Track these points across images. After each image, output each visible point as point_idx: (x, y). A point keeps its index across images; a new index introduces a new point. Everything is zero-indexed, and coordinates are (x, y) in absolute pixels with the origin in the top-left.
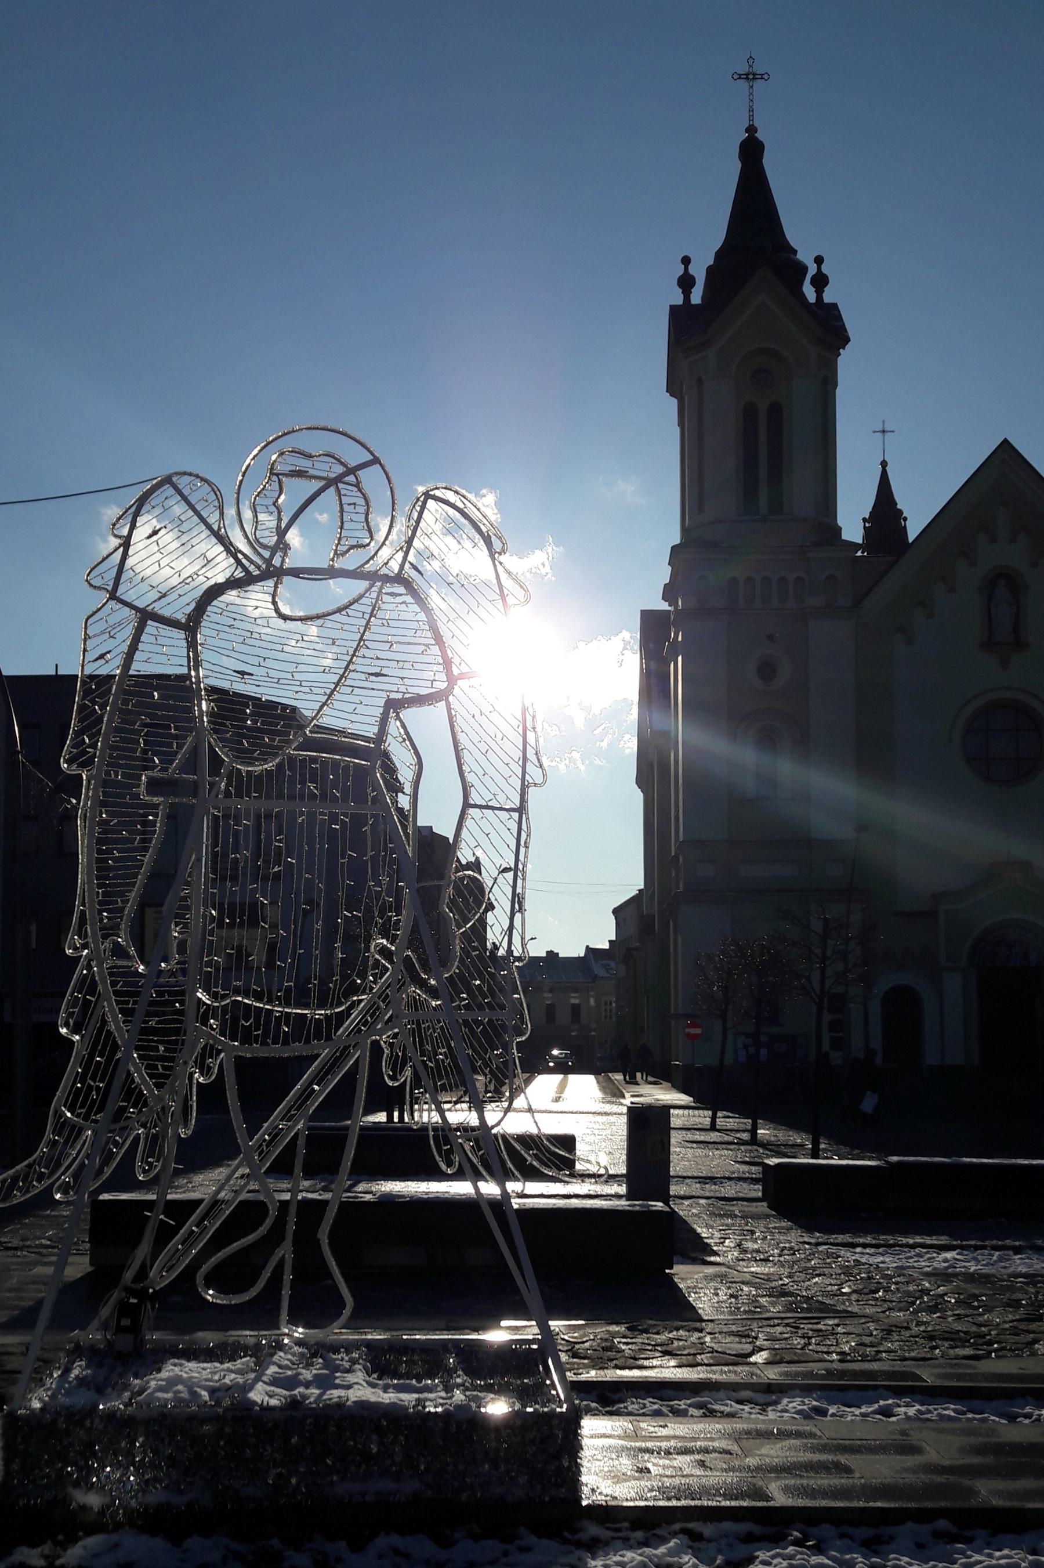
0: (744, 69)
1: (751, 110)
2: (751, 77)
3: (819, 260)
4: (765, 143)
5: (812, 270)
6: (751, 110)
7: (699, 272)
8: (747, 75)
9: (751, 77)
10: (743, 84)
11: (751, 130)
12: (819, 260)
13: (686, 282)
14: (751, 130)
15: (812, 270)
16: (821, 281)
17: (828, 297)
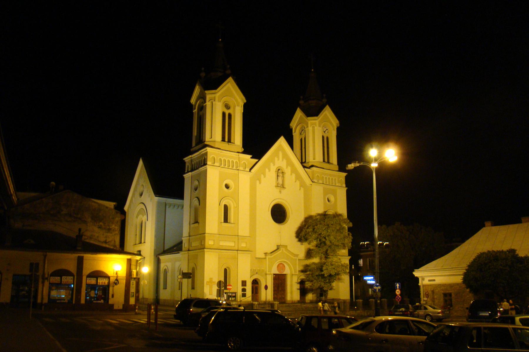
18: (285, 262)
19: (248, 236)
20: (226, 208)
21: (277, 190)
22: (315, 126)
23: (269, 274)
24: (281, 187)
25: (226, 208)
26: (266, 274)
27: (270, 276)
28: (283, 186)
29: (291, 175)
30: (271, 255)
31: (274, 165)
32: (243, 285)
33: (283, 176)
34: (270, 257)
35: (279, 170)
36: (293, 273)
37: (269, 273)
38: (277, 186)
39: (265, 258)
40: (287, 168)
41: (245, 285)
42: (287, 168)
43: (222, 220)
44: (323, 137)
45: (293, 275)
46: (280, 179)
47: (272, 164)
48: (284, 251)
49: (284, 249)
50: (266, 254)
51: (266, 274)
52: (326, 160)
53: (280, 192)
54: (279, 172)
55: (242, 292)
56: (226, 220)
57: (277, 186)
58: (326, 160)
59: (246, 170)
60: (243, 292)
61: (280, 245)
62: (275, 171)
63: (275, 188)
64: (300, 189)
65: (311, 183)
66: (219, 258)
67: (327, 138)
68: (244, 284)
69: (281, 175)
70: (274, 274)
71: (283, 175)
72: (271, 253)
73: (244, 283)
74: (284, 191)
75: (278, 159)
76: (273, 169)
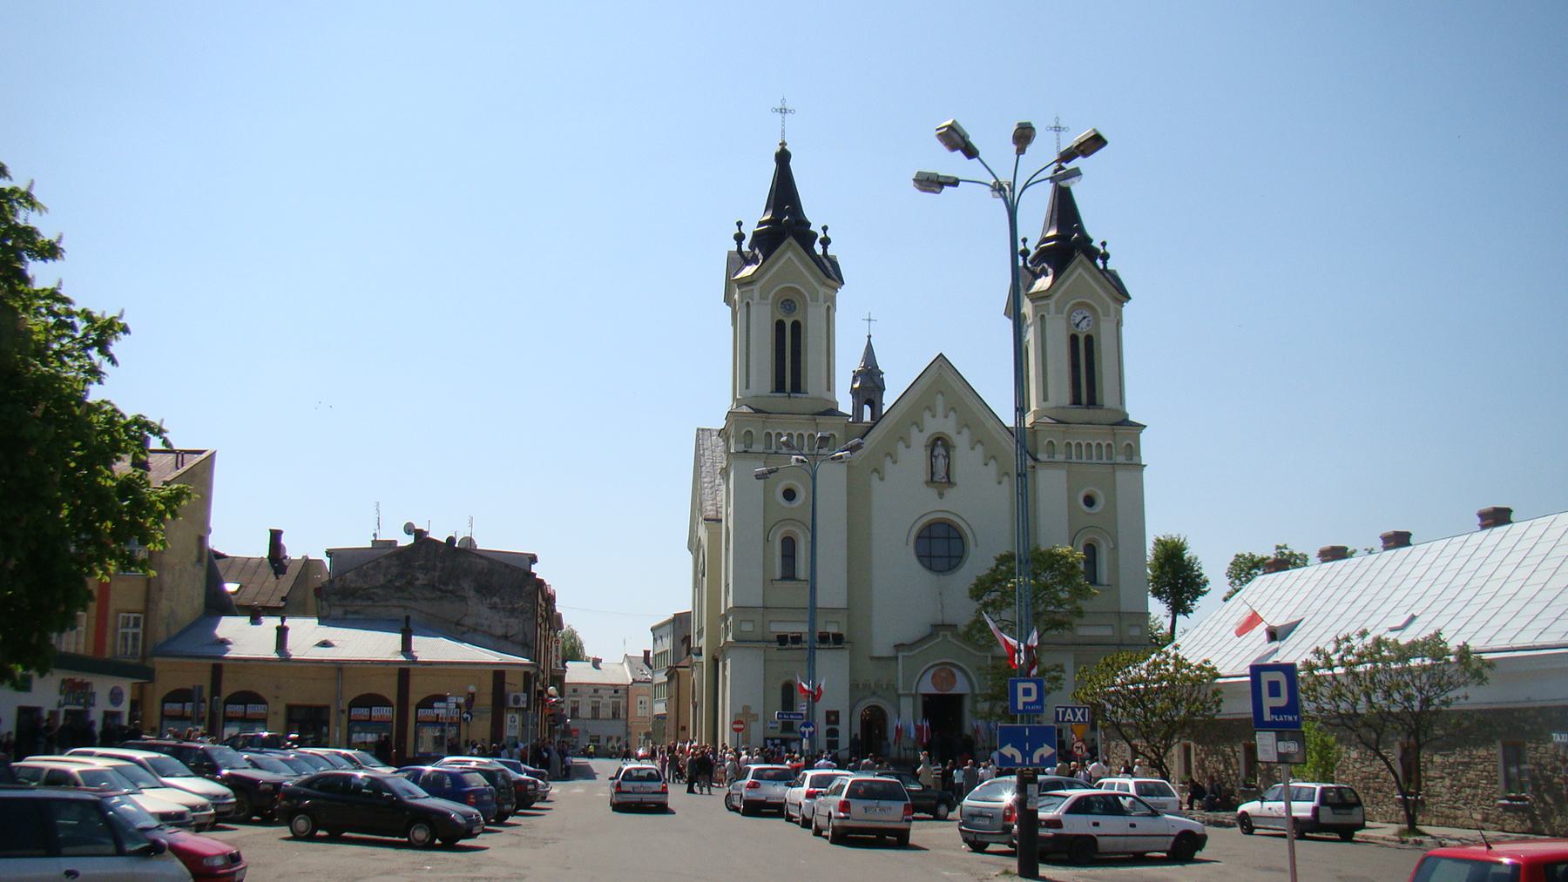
0: (779, 106)
1: (783, 131)
2: (783, 111)
3: (825, 229)
5: (821, 235)
6: (783, 131)
7: (749, 231)
8: (781, 109)
9: (783, 111)
10: (779, 115)
11: (783, 144)
12: (825, 229)
13: (739, 238)
14: (783, 144)
15: (821, 235)
16: (826, 242)
17: (830, 252)
18: (961, 669)
19: (845, 607)
20: (789, 545)
21: (932, 493)
22: (1045, 314)
23: (905, 695)
24: (941, 482)
25: (789, 545)
26: (899, 696)
27: (911, 699)
28: (949, 482)
29: (972, 448)
30: (911, 651)
32: (828, 722)
33: (948, 456)
34: (906, 654)
35: (938, 439)
36: (977, 692)
37: (906, 692)
39: (897, 657)
40: (959, 433)
41: (837, 722)
42: (959, 433)
43: (778, 574)
44: (1074, 339)
45: (976, 696)
46: (941, 463)
47: (914, 430)
48: (949, 636)
49: (948, 634)
50: (899, 647)
51: (899, 696)
53: (941, 495)
54: (939, 443)
55: (827, 736)
56: (789, 574)
57: (931, 481)
60: (829, 738)
61: (941, 623)
62: (925, 444)
63: (925, 486)
64: (1000, 483)
66: (765, 660)
67: (1089, 340)
68: (833, 718)
69: (940, 451)
70: (924, 695)
71: (948, 453)
72: (912, 644)
73: (833, 717)
74: (950, 493)
75: (934, 416)
76: (919, 440)
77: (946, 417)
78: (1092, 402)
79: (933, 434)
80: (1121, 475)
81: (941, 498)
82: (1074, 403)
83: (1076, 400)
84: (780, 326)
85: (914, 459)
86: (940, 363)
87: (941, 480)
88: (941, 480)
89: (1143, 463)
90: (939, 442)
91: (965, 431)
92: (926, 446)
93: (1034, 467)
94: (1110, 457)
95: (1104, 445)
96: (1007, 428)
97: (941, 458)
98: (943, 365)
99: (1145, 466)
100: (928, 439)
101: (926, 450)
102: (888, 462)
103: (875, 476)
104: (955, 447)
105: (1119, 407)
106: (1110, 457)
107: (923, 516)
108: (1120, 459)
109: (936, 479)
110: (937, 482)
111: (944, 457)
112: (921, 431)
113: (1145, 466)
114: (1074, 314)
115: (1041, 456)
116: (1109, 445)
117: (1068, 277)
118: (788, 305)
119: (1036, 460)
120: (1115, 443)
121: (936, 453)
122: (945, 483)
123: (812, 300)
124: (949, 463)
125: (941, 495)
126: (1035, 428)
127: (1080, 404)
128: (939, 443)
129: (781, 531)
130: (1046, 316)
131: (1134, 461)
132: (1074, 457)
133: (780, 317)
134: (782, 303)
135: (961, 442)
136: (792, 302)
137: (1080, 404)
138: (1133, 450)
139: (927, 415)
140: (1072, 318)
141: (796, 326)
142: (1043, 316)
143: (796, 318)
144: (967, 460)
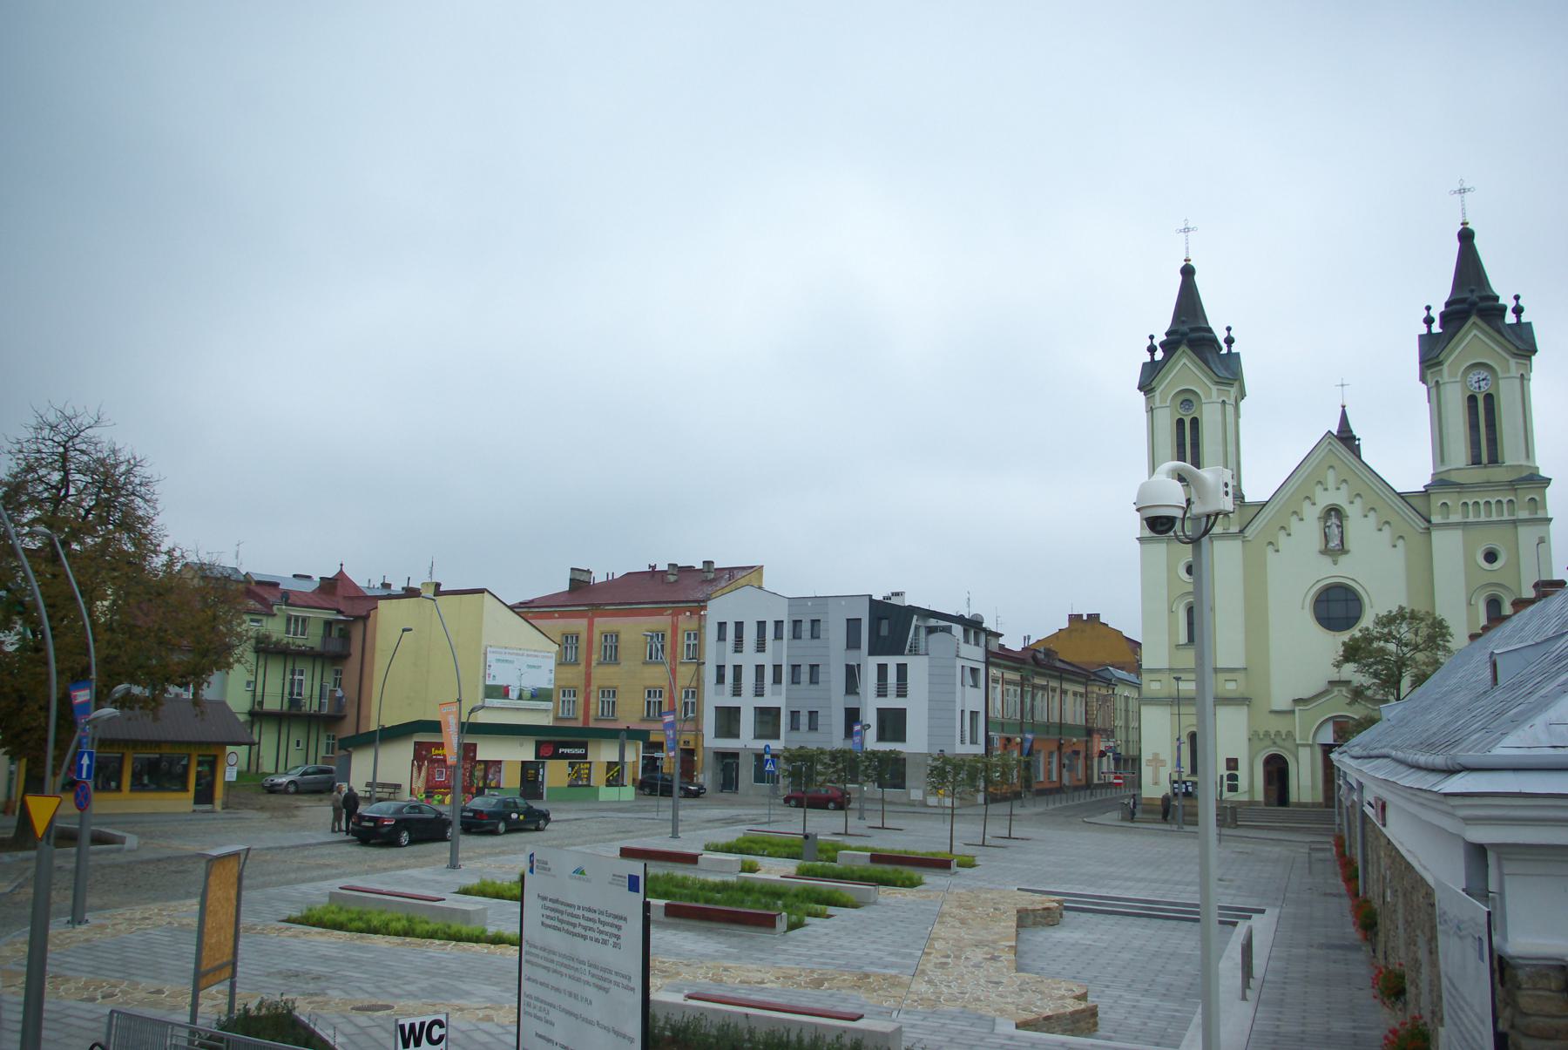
4: (1179, 269)
21: (1327, 560)
22: (1439, 379)
28: (1342, 549)
31: (1314, 504)
33: (1340, 526)
35: (1332, 509)
38: (1326, 551)
40: (1352, 503)
44: (1472, 399)
52: (1485, 458)
53: (1335, 563)
57: (1326, 551)
58: (1485, 458)
59: (1231, 531)
65: (1426, 525)
67: (1489, 398)
69: (1334, 520)
71: (1341, 523)
74: (1343, 559)
76: (1312, 513)
77: (1338, 489)
78: (1494, 459)
79: (1325, 507)
80: (1523, 531)
81: (1335, 564)
82: (1473, 464)
83: (1476, 461)
84: (1180, 422)
85: (1308, 531)
86: (1330, 440)
87: (1335, 549)
88: (1335, 549)
89: (1549, 516)
90: (1333, 513)
91: (1358, 501)
92: (1319, 518)
93: (1429, 529)
94: (1512, 512)
95: (1505, 500)
96: (1399, 494)
97: (1334, 526)
98: (1332, 442)
99: (1550, 520)
100: (1321, 512)
101: (1319, 522)
102: (1282, 534)
103: (1270, 549)
104: (1347, 517)
105: (1523, 462)
106: (1512, 512)
107: (1318, 581)
108: (1523, 514)
109: (1329, 546)
110: (1331, 551)
111: (1338, 526)
112: (1314, 504)
113: (1550, 520)
114: (1471, 375)
115: (1435, 519)
116: (1510, 501)
117: (1462, 339)
118: (1187, 403)
119: (1429, 521)
120: (1517, 498)
121: (1328, 524)
122: (1339, 550)
123: (1206, 398)
124: (1342, 532)
125: (1335, 563)
126: (1429, 492)
127: (1480, 463)
128: (1334, 511)
129: (1183, 604)
130: (1441, 382)
131: (1540, 514)
132: (1471, 514)
133: (1180, 417)
134: (1182, 403)
135: (1353, 511)
136: (1191, 401)
137: (1480, 463)
138: (1537, 504)
139: (1319, 489)
140: (1469, 379)
141: (1195, 422)
142: (1437, 382)
143: (1194, 415)
144: (1360, 528)
